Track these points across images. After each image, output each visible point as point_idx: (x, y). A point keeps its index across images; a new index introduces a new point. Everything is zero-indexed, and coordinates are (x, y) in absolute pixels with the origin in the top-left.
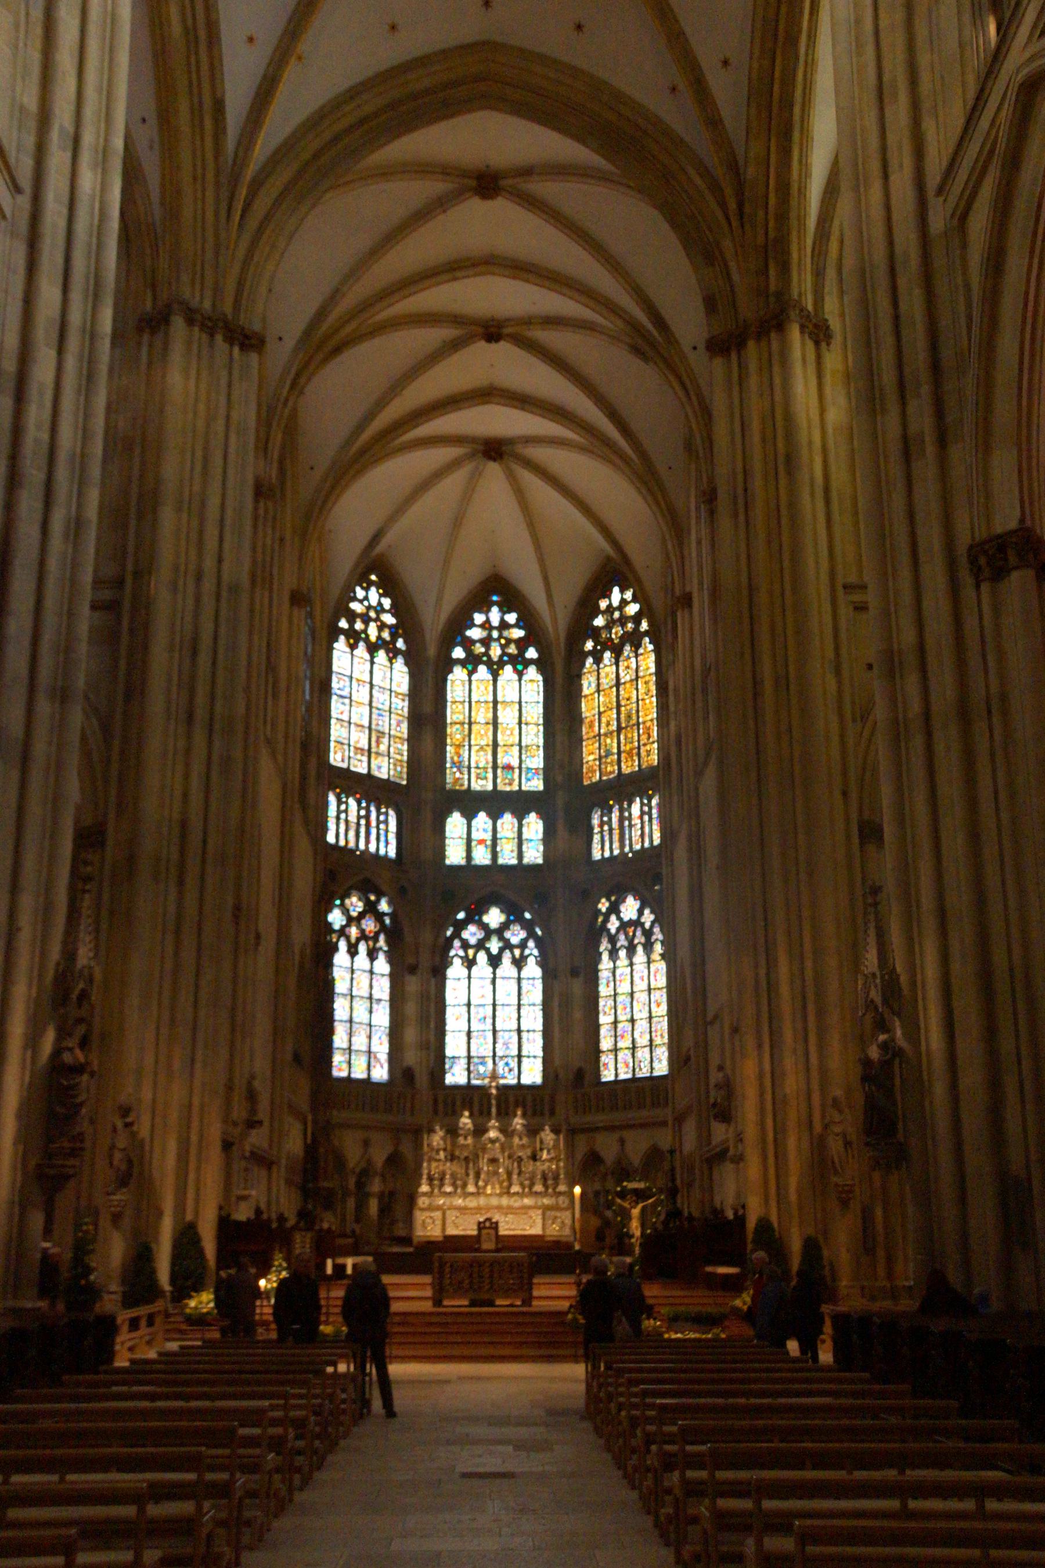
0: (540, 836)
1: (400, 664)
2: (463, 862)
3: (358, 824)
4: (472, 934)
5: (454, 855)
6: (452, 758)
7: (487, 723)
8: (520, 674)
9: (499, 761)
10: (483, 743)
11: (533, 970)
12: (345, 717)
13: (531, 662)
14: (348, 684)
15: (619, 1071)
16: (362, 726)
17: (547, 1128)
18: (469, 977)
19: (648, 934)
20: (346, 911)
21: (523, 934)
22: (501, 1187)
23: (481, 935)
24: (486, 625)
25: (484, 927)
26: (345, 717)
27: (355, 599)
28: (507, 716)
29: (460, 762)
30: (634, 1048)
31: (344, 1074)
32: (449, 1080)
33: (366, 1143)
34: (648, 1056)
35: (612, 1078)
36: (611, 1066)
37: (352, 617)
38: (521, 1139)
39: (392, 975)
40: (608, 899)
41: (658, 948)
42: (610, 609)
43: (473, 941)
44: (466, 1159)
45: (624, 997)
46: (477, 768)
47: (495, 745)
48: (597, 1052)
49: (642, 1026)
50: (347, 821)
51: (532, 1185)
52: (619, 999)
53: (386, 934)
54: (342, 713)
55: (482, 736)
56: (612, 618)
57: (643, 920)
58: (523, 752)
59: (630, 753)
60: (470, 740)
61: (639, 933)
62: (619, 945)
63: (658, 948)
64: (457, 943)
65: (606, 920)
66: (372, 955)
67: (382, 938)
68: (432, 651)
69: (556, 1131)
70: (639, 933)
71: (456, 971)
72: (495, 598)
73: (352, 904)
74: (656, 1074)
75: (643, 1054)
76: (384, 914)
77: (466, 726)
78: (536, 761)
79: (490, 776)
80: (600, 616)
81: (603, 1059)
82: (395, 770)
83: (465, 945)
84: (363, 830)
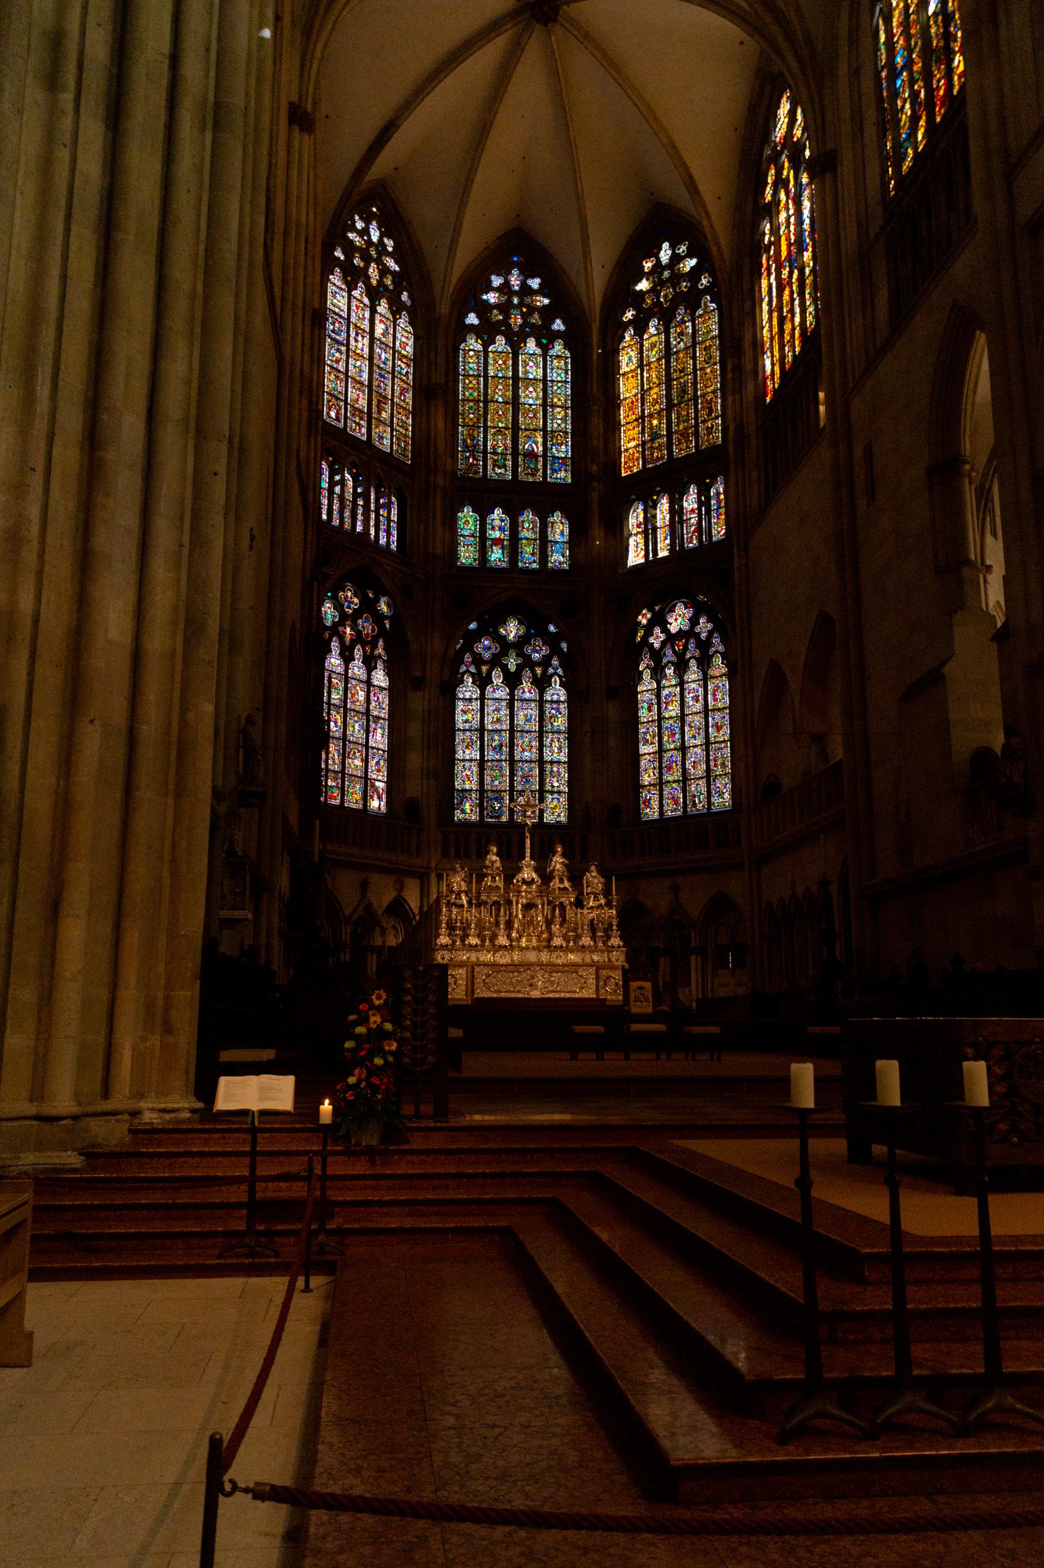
0: (566, 538)
1: (403, 322)
2: (475, 564)
3: (354, 503)
4: (485, 646)
5: (467, 555)
6: (465, 441)
7: (506, 403)
8: (545, 349)
9: (520, 447)
10: (500, 425)
11: (557, 692)
12: (341, 367)
13: (558, 334)
14: (344, 328)
15: (665, 808)
16: (361, 383)
17: (593, 868)
18: (482, 698)
19: (704, 646)
20: (338, 606)
21: (545, 651)
22: (539, 940)
23: (496, 649)
24: (505, 289)
25: (502, 640)
26: (341, 367)
27: (353, 229)
28: (530, 397)
29: (474, 446)
30: (685, 780)
31: (338, 802)
32: (458, 815)
33: (364, 886)
34: (704, 790)
35: (656, 816)
36: (655, 804)
37: (350, 248)
38: (561, 881)
39: (391, 690)
40: (651, 610)
41: (718, 660)
42: (658, 267)
43: (487, 655)
44: (495, 903)
45: (671, 721)
46: (495, 453)
47: (515, 428)
48: (637, 786)
49: (696, 754)
50: (342, 497)
51: (578, 937)
52: (666, 724)
53: (384, 642)
54: (337, 361)
55: (499, 418)
56: (660, 279)
57: (697, 630)
58: (549, 439)
59: (684, 435)
60: (485, 421)
61: (691, 646)
62: (665, 661)
63: (718, 660)
64: (468, 658)
65: (649, 630)
66: (369, 664)
67: (381, 643)
68: (444, 309)
69: (603, 872)
70: (691, 646)
71: (468, 689)
72: (515, 259)
73: (346, 597)
74: (714, 809)
75: (697, 788)
76: (383, 617)
77: (481, 405)
78: (563, 451)
79: (509, 463)
80: (644, 281)
81: (644, 794)
82: (399, 445)
83: (478, 661)
84: (360, 511)
